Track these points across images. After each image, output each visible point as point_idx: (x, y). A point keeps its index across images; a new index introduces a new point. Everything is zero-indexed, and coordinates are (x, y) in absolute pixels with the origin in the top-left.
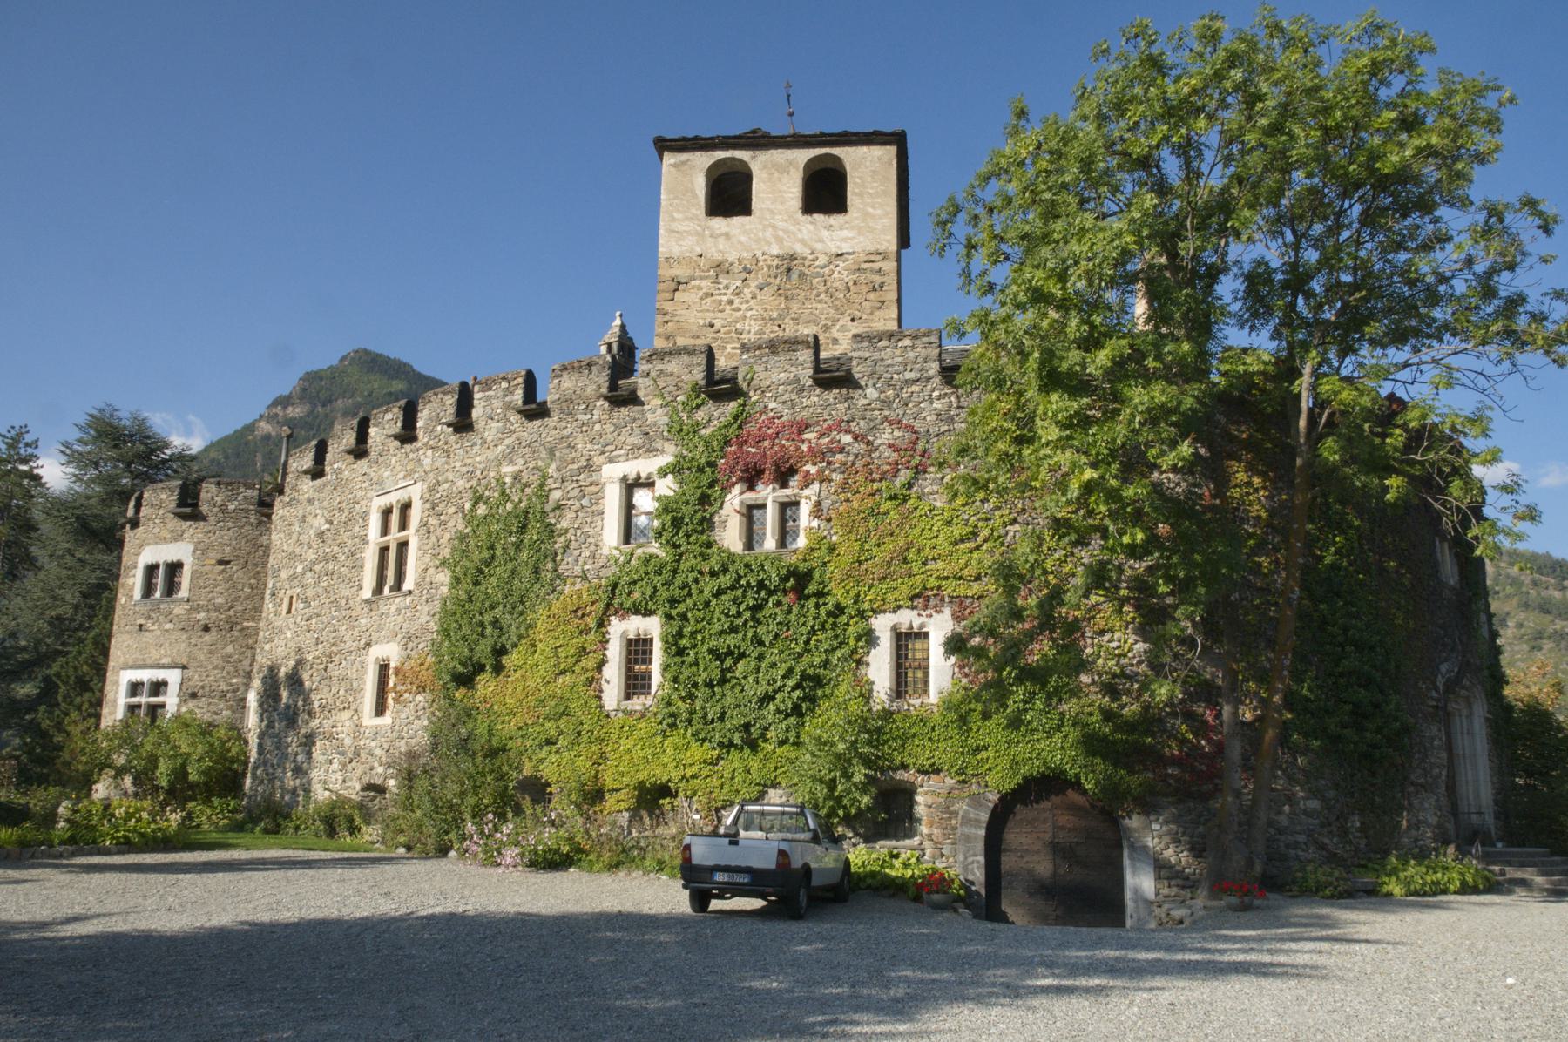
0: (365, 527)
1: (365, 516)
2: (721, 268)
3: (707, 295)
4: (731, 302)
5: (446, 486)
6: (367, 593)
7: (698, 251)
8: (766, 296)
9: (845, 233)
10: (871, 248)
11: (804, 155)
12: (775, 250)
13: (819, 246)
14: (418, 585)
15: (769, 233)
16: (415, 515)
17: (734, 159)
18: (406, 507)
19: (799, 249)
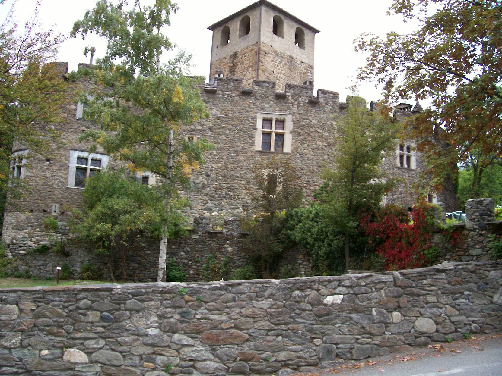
0: (255, 124)
1: (254, 118)
2: (276, 53)
3: (272, 61)
4: (278, 66)
5: (308, 121)
6: (258, 146)
7: (271, 44)
8: (286, 68)
9: (304, 56)
10: (309, 64)
11: (296, 26)
12: (288, 53)
13: (298, 57)
14: (292, 152)
15: (287, 47)
16: (289, 125)
17: (279, 17)
18: (281, 122)
19: (294, 56)
